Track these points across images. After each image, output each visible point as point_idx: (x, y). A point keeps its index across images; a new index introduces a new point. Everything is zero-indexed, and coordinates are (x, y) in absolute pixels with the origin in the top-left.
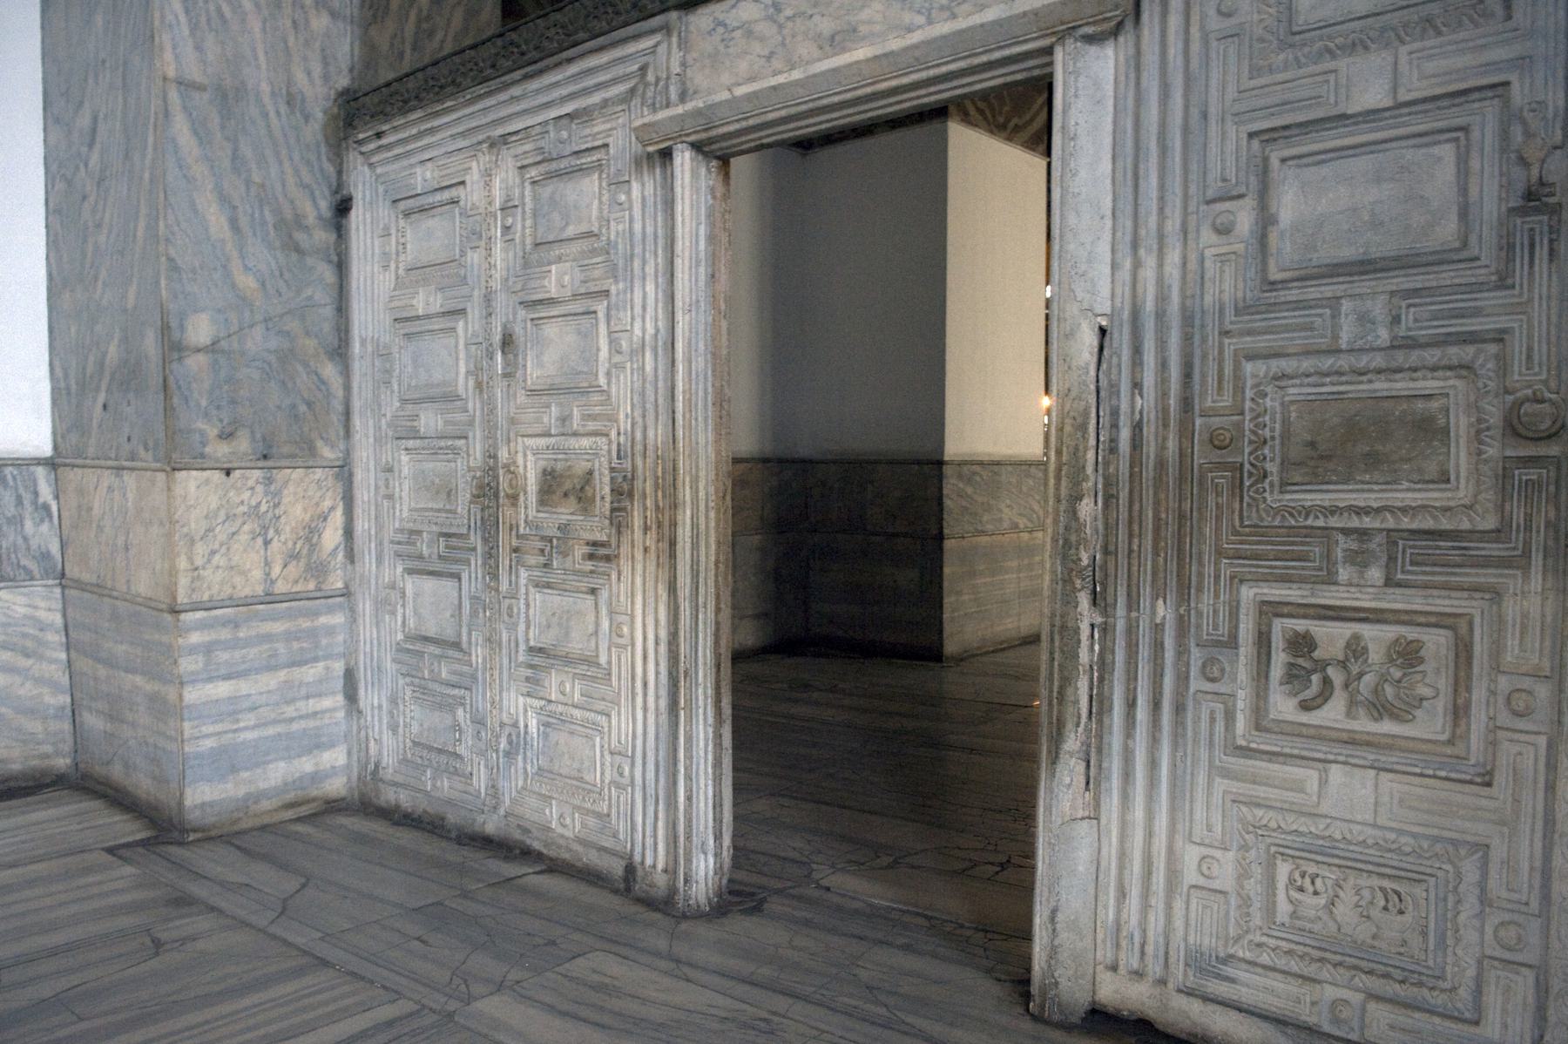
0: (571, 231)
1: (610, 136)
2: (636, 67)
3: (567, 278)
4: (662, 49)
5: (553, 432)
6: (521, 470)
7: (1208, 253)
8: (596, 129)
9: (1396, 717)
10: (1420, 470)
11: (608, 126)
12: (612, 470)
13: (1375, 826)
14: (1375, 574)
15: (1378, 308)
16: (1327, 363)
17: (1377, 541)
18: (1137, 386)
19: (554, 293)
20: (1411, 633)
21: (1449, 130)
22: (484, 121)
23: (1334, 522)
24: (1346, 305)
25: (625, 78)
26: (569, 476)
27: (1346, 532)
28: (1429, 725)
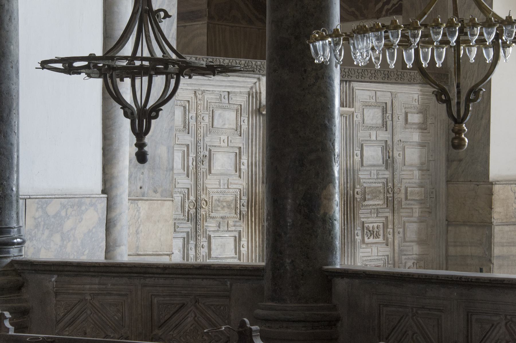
0: (227, 126)
1: (242, 103)
2: (250, 86)
3: (226, 141)
4: (257, 84)
5: (221, 187)
6: (207, 199)
7: (356, 159)
8: (238, 99)
9: (378, 238)
10: (379, 198)
11: (242, 100)
12: (240, 199)
13: (378, 256)
14: (375, 215)
15: (375, 172)
16: (371, 181)
17: (376, 211)
18: (347, 182)
19: (222, 144)
20: (379, 224)
21: (381, 146)
22: (197, 83)
23: (370, 207)
24: (372, 171)
25: (247, 87)
26: (225, 202)
27: (373, 208)
28: (381, 239)
